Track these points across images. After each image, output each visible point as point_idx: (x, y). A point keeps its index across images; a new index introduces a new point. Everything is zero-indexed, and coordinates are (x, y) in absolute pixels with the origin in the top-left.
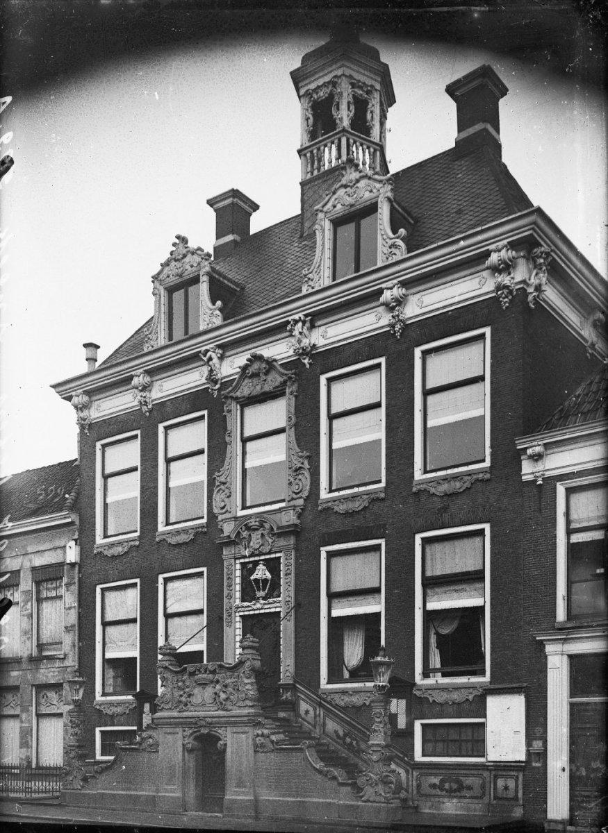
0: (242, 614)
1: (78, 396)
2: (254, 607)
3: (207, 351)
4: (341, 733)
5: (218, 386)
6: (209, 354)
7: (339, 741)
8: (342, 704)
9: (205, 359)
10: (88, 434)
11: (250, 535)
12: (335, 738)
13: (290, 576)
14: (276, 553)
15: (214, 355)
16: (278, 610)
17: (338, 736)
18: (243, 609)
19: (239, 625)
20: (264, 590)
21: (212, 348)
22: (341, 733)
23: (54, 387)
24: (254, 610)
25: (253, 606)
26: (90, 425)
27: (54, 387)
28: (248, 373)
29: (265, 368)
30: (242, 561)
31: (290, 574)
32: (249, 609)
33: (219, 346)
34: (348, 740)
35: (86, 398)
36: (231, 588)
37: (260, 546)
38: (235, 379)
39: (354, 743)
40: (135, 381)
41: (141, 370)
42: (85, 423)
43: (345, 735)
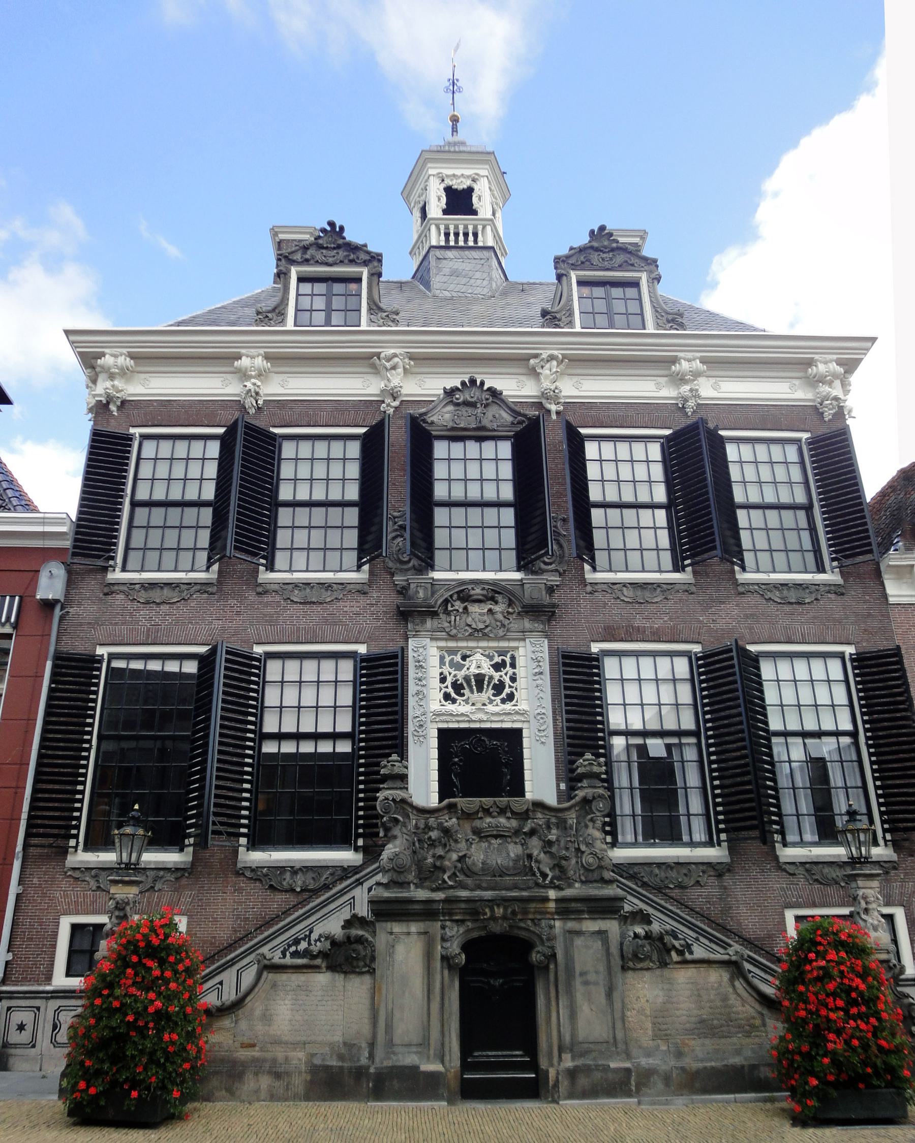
0: (445, 726)
1: (115, 356)
3: (395, 355)
5: (396, 403)
6: (396, 360)
9: (388, 365)
10: (115, 414)
11: (465, 608)
13: (542, 676)
14: (509, 640)
15: (401, 364)
19: (434, 743)
21: (400, 354)
23: (68, 333)
24: (469, 721)
26: (124, 402)
27: (68, 333)
28: (457, 399)
29: (487, 399)
30: (442, 644)
31: (541, 673)
33: (412, 357)
35: (130, 362)
36: (424, 682)
38: (433, 401)
40: (245, 362)
41: (262, 351)
42: (118, 395)
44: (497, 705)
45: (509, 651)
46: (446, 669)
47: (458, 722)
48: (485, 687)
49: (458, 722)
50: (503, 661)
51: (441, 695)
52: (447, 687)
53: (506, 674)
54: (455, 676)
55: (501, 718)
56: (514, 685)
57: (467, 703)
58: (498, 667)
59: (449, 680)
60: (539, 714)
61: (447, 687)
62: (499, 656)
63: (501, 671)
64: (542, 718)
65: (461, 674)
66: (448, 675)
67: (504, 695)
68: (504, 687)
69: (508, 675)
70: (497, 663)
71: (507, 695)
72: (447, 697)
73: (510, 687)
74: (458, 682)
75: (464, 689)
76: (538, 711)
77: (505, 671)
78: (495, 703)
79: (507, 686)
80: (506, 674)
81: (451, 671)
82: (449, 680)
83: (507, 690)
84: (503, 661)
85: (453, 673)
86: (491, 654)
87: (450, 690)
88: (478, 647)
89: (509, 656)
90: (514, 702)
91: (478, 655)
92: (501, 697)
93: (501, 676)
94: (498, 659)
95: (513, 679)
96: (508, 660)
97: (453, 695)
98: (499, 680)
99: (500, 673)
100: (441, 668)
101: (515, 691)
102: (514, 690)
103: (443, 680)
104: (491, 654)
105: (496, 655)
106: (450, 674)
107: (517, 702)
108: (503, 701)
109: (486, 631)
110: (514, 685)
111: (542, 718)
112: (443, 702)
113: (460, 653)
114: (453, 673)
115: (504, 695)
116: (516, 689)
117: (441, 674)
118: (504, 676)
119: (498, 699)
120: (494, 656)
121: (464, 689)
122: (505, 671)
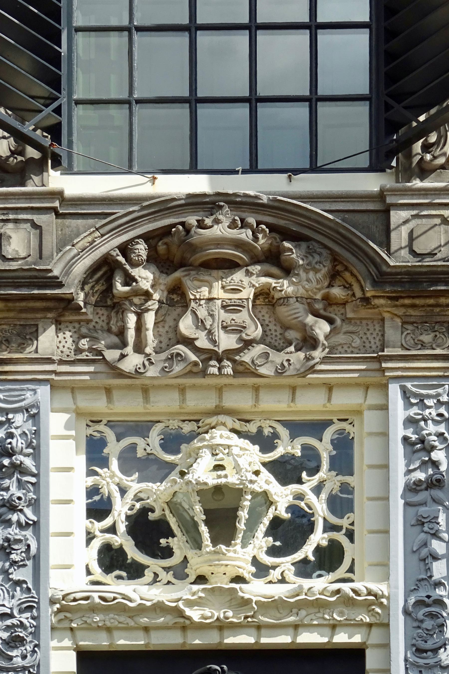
48: (241, 526)
52: (112, 530)
53: (317, 490)
56: (345, 522)
61: (112, 530)
62: (293, 437)
63: (300, 481)
64: (432, 616)
66: (116, 495)
68: (311, 528)
74: (152, 516)
75: (170, 534)
78: (275, 575)
79: (320, 526)
81: (126, 480)
86: (267, 431)
90: (341, 572)
92: (298, 556)
98: (291, 508)
99: (294, 487)
100: (91, 473)
102: (341, 537)
104: (267, 431)
105: (284, 432)
106: (123, 491)
107: (351, 570)
110: (345, 522)
111: (432, 616)
113: (158, 428)
116: (350, 535)
118: (311, 497)
120: (275, 435)
121: (170, 534)
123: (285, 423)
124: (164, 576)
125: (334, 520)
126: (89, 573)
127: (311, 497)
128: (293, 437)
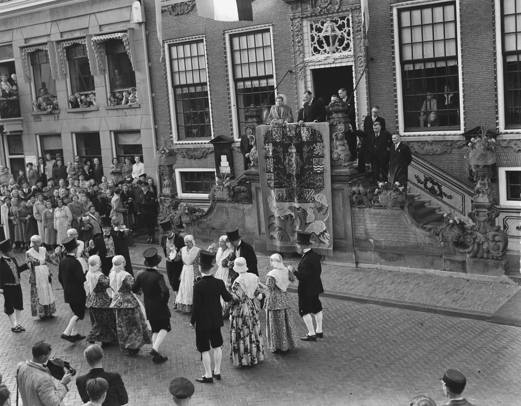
0: (313, 68)
2: (326, 62)
4: (422, 179)
7: (420, 185)
8: (421, 152)
12: (416, 181)
13: (360, 32)
16: (349, 64)
17: (419, 181)
18: (314, 64)
19: (309, 78)
20: (334, 44)
22: (422, 179)
25: (323, 61)
32: (320, 63)
34: (429, 185)
37: (328, 5)
39: (436, 187)
43: (426, 180)
44: (341, 52)
45: (346, 17)
46: (314, 32)
47: (320, 65)
49: (320, 65)
50: (343, 23)
51: (312, 49)
52: (315, 44)
54: (319, 36)
55: (340, 61)
57: (326, 52)
58: (340, 28)
59: (316, 39)
60: (359, 57)
61: (315, 44)
62: (341, 20)
63: (342, 30)
64: (361, 59)
65: (322, 35)
67: (344, 45)
69: (346, 32)
70: (340, 25)
71: (346, 45)
72: (316, 50)
73: (348, 39)
76: (358, 55)
77: (344, 30)
78: (339, 51)
79: (346, 39)
80: (345, 32)
81: (316, 33)
82: (316, 39)
83: (346, 42)
84: (343, 23)
85: (318, 34)
86: (337, 19)
87: (317, 45)
88: (327, 17)
89: (346, 19)
91: (328, 22)
93: (342, 33)
94: (340, 22)
95: (349, 34)
96: (345, 22)
97: (318, 48)
98: (341, 36)
99: (342, 31)
101: (349, 42)
103: (313, 39)
104: (337, 19)
105: (339, 20)
106: (316, 35)
108: (344, 49)
109: (328, 8)
112: (314, 53)
113: (320, 21)
114: (318, 34)
115: (344, 45)
117: (312, 35)
118: (344, 33)
119: (341, 48)
120: (338, 20)
122: (344, 30)
123: (339, 18)
124: (323, 52)
125: (348, 38)
126: (312, 53)
127: (344, 33)
128: (341, 20)
